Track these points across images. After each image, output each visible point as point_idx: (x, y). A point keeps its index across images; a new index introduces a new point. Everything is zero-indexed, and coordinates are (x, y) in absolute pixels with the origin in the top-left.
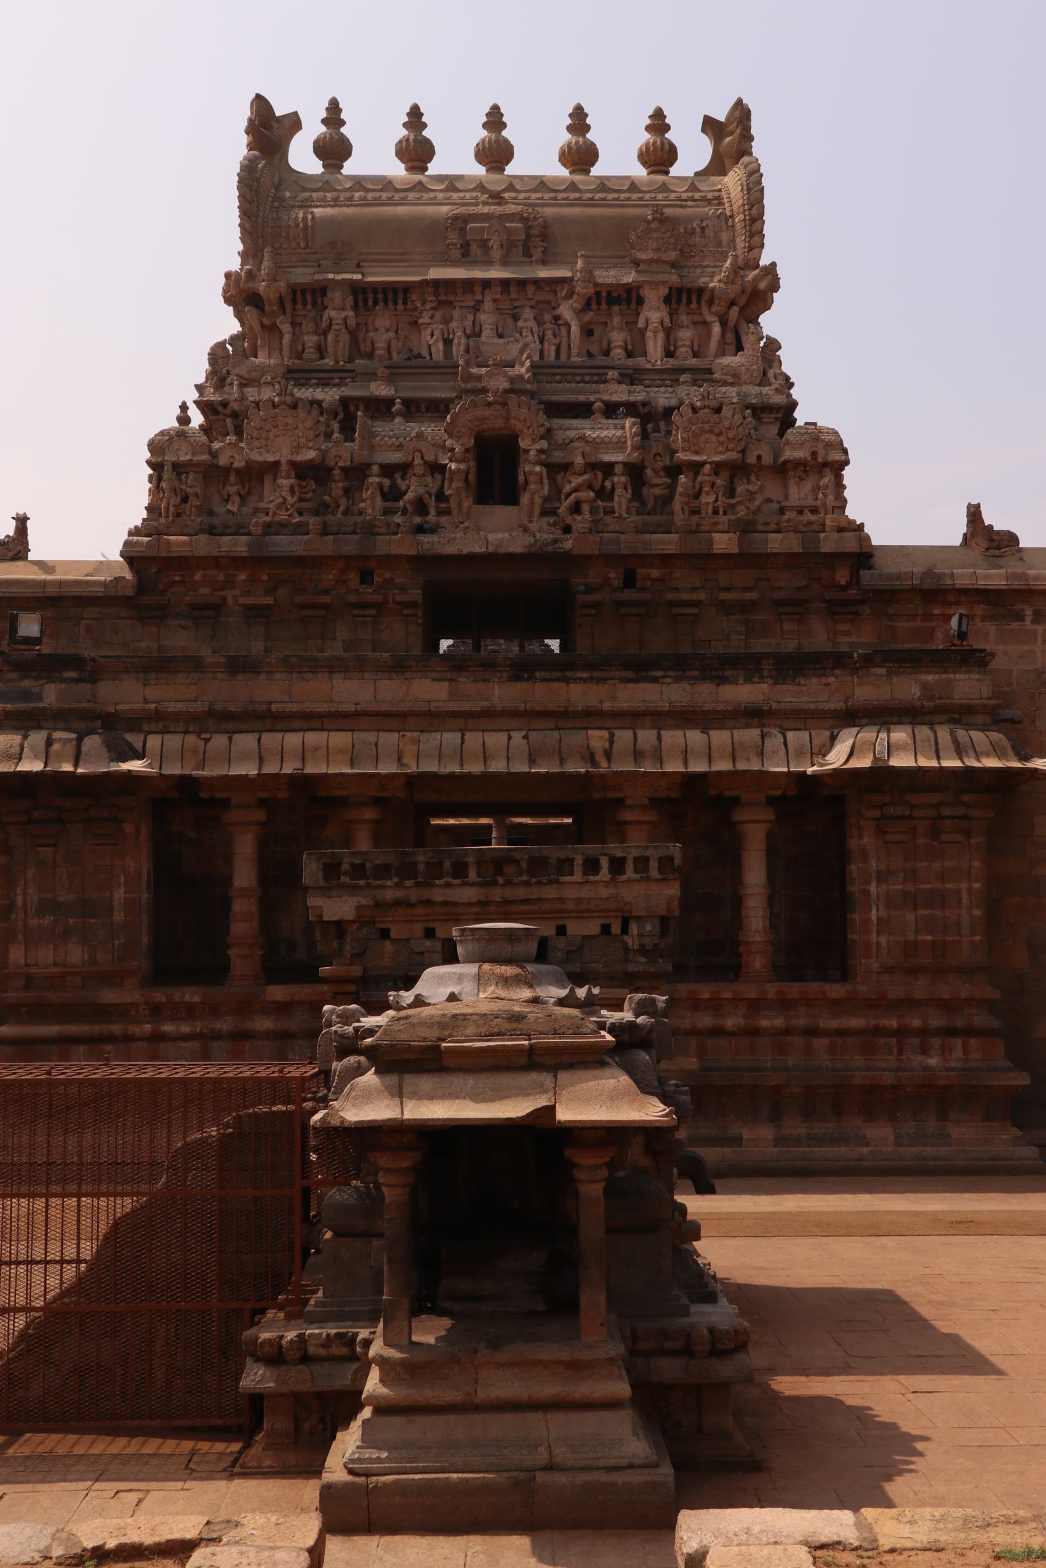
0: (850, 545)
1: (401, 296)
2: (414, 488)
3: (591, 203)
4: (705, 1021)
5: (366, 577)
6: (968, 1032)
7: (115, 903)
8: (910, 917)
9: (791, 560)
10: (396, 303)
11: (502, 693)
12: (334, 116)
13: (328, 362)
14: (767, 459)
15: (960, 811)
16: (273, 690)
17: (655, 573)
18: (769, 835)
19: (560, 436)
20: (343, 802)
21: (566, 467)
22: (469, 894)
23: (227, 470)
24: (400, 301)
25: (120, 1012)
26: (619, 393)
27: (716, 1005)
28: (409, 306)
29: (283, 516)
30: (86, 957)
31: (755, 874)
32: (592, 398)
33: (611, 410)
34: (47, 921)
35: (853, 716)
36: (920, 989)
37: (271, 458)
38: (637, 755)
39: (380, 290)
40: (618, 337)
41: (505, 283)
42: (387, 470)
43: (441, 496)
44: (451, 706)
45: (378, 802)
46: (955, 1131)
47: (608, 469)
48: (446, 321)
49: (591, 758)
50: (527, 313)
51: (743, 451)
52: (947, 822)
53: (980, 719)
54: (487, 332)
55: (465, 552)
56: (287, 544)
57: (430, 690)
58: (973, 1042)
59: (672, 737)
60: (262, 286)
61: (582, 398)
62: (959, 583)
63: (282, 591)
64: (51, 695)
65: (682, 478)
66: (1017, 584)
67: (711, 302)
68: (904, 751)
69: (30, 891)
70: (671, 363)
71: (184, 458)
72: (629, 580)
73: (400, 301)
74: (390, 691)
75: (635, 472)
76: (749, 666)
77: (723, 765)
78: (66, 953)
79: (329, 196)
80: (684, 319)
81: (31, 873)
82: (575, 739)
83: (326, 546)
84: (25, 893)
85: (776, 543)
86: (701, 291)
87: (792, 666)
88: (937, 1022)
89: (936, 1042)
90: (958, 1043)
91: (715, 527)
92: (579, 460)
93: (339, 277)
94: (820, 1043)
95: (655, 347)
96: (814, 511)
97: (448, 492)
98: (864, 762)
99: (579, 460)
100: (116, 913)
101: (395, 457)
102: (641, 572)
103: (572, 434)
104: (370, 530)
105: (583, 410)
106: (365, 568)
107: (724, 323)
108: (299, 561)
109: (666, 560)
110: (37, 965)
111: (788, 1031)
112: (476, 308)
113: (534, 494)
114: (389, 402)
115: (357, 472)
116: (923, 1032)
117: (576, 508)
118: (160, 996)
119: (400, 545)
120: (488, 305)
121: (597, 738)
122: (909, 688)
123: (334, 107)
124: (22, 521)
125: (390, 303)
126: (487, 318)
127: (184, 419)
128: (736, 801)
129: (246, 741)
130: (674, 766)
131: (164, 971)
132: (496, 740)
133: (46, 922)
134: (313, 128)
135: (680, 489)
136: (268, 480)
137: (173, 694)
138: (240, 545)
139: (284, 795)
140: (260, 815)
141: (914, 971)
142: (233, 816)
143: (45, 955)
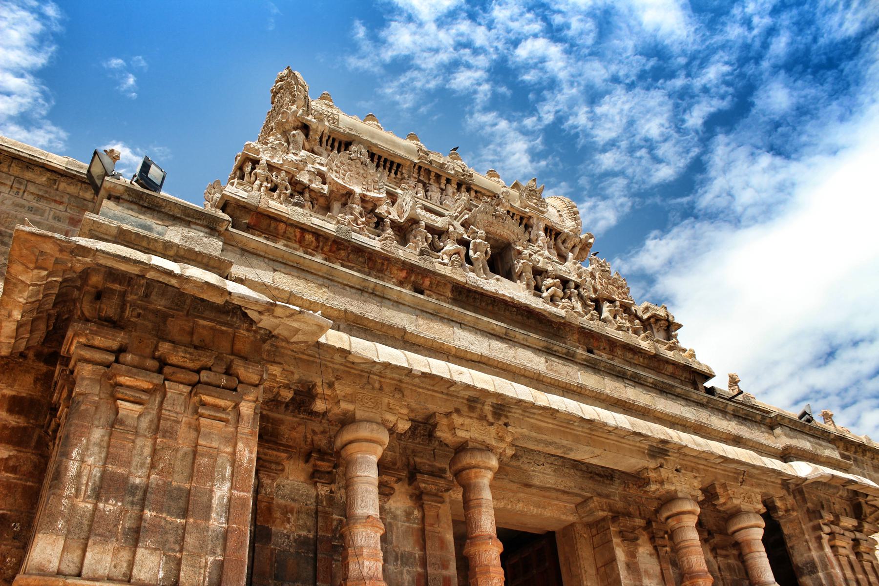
1: (395, 167)
7: (215, 502)
10: (390, 171)
24: (393, 171)
28: (399, 176)
30: (161, 574)
34: (109, 507)
39: (382, 160)
55: (500, 292)
67: (564, 242)
69: (90, 460)
73: (393, 171)
78: (131, 564)
81: (98, 434)
84: (82, 461)
100: (213, 515)
110: (79, 575)
125: (387, 170)
133: (109, 507)
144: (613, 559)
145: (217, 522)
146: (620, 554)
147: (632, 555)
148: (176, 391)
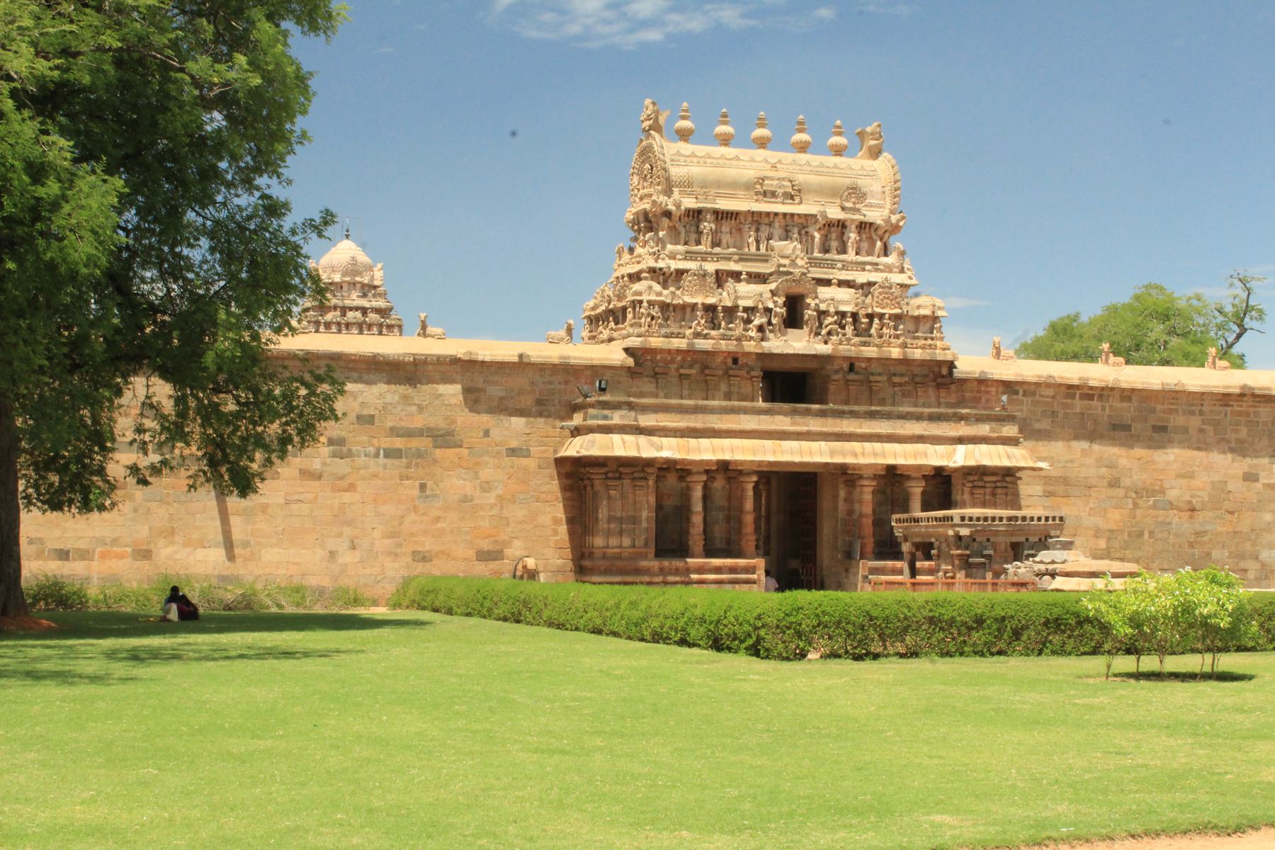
2: (758, 320)
3: (818, 173)
5: (735, 361)
11: (815, 425)
13: (701, 248)
15: (1004, 484)
17: (863, 365)
18: (923, 493)
19: (820, 296)
20: (741, 472)
23: (668, 305)
25: (647, 572)
26: (844, 276)
29: (699, 329)
32: (831, 277)
33: (841, 283)
34: (613, 526)
37: (694, 301)
38: (875, 455)
41: (785, 215)
42: (746, 309)
43: (770, 323)
44: (792, 428)
47: (843, 315)
48: (757, 230)
49: (855, 455)
52: (999, 491)
54: (776, 237)
57: (782, 422)
60: (671, 207)
61: (826, 277)
62: (996, 377)
64: (617, 418)
65: (876, 321)
66: (1019, 379)
70: (860, 259)
71: (653, 297)
72: (852, 368)
75: (855, 316)
77: (911, 462)
79: (695, 160)
81: (605, 502)
86: (871, 224)
91: (889, 344)
92: (832, 310)
93: (709, 206)
96: (932, 339)
97: (774, 321)
98: (972, 463)
99: (832, 310)
101: (749, 303)
102: (857, 364)
103: (828, 296)
104: (739, 339)
105: (827, 283)
108: (706, 353)
109: (869, 360)
112: (770, 225)
114: (740, 273)
117: (829, 333)
118: (666, 563)
120: (777, 225)
121: (856, 446)
126: (777, 232)
129: (705, 442)
131: (661, 553)
132: (815, 445)
135: (875, 326)
136: (688, 310)
138: (680, 344)
139: (714, 468)
140: (704, 478)
142: (695, 478)
143: (613, 541)
144: (837, 496)
145: (644, 525)
146: (842, 494)
147: (850, 494)
148: (626, 482)
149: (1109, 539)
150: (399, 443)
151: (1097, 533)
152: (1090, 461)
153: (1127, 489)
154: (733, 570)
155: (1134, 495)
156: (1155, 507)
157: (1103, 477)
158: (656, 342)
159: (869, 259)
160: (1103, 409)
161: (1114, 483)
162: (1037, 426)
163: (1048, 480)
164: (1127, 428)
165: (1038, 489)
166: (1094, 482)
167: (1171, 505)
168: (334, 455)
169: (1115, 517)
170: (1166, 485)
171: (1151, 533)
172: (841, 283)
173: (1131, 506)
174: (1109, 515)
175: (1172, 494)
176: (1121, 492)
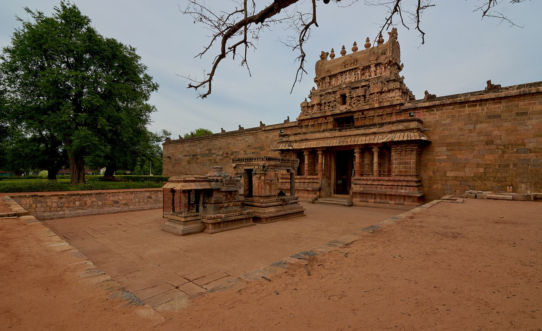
0: (399, 102)
2: (331, 105)
4: (365, 182)
6: (411, 186)
8: (401, 166)
9: (389, 107)
11: (337, 134)
12: (333, 51)
14: (386, 90)
16: (308, 136)
21: (353, 97)
22: (244, 163)
26: (363, 84)
27: (367, 180)
31: (376, 160)
35: (391, 132)
36: (402, 178)
40: (367, 74)
41: (350, 70)
42: (329, 103)
45: (322, 151)
46: (405, 203)
47: (359, 96)
50: (353, 73)
51: (382, 90)
53: (415, 131)
56: (315, 116)
57: (327, 134)
58: (411, 188)
59: (360, 138)
63: (316, 123)
64: (284, 139)
68: (398, 137)
72: (363, 114)
74: (322, 135)
76: (374, 125)
77: (367, 142)
80: (378, 68)
82: (346, 140)
83: (319, 115)
85: (385, 104)
87: (382, 125)
88: (404, 184)
89: (404, 187)
90: (408, 188)
92: (354, 96)
94: (383, 187)
95: (373, 75)
99: (354, 96)
105: (358, 88)
106: (325, 117)
107: (385, 68)
109: (368, 110)
111: (378, 185)
113: (349, 102)
115: (325, 103)
116: (402, 186)
119: (329, 113)
121: (349, 140)
122: (401, 127)
123: (333, 49)
124: (288, 117)
127: (306, 100)
128: (373, 148)
130: (359, 143)
134: (330, 53)
137: (298, 138)
138: (309, 117)
141: (401, 175)
149: (485, 168)
150: (254, 151)
151: (478, 166)
152: (473, 134)
153: (498, 145)
154: (313, 179)
155: (503, 147)
156: (517, 152)
157: (482, 141)
158: (302, 118)
159: (380, 75)
160: (483, 110)
161: (489, 143)
162: (444, 122)
163: (449, 144)
164: (500, 116)
165: (445, 149)
166: (476, 143)
167: (530, 151)
168: (245, 154)
169: (489, 158)
170: (525, 141)
171: (515, 165)
172: (362, 87)
173: (500, 152)
174: (486, 157)
175: (531, 146)
176: (494, 147)
